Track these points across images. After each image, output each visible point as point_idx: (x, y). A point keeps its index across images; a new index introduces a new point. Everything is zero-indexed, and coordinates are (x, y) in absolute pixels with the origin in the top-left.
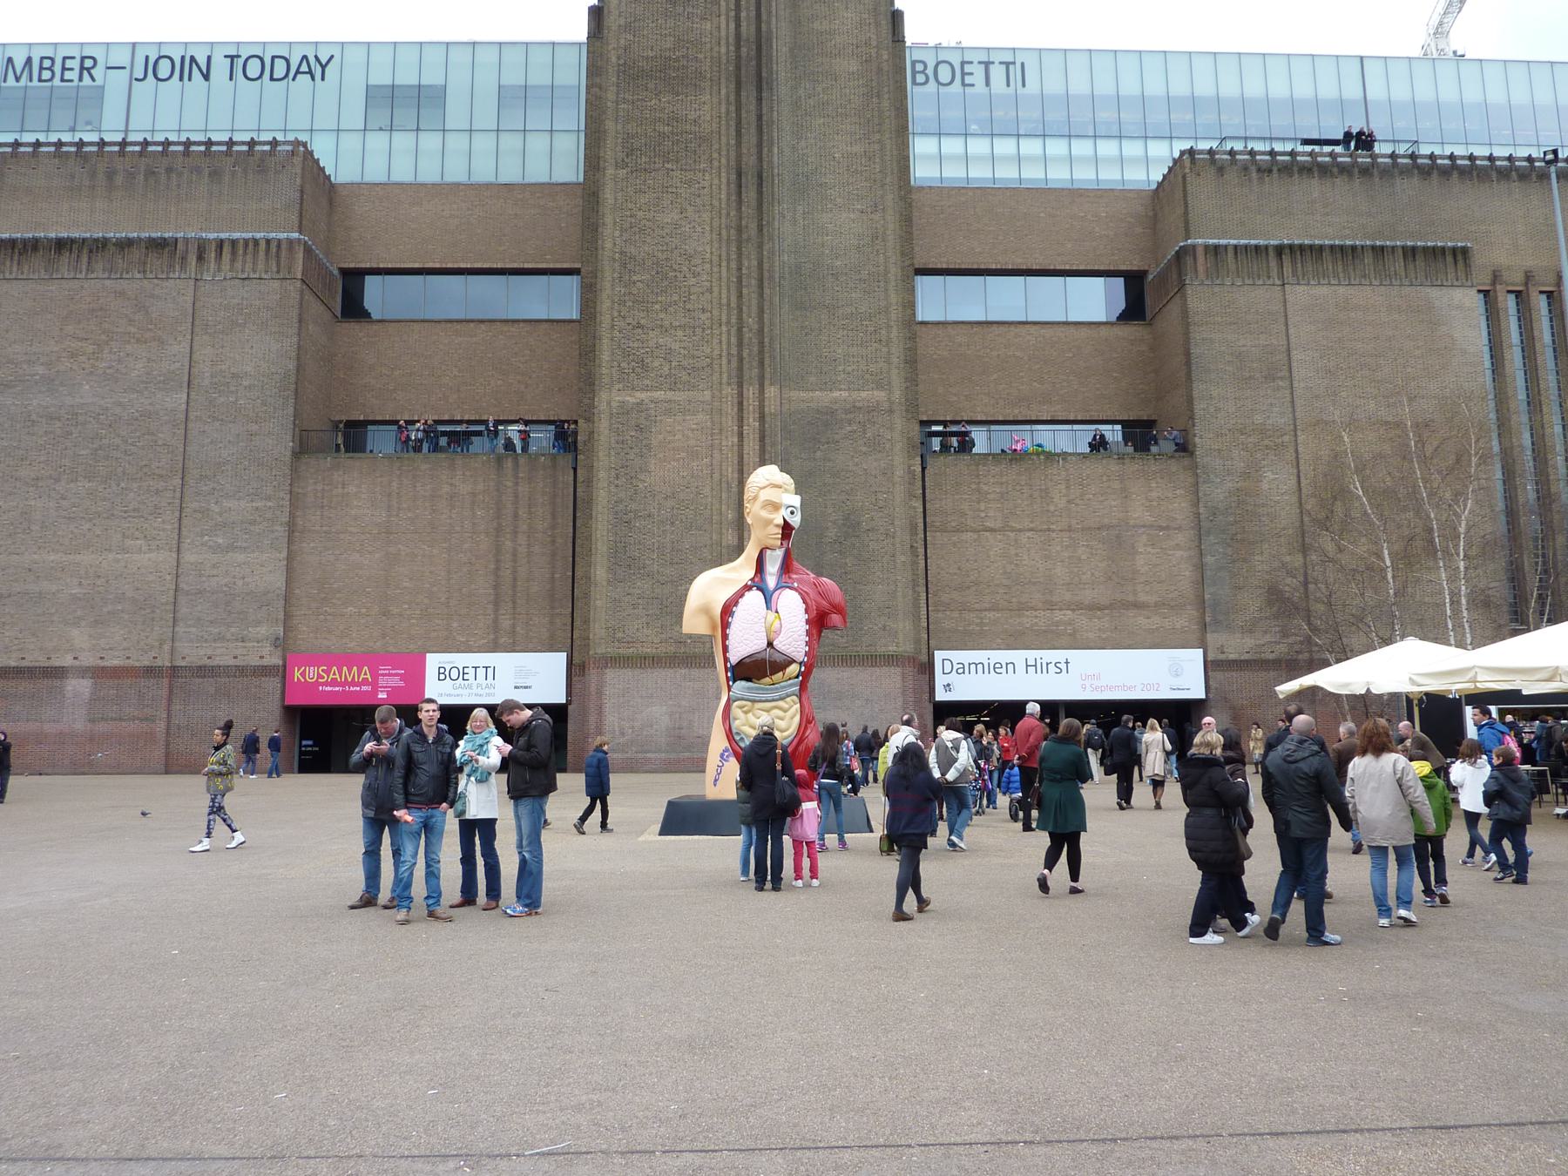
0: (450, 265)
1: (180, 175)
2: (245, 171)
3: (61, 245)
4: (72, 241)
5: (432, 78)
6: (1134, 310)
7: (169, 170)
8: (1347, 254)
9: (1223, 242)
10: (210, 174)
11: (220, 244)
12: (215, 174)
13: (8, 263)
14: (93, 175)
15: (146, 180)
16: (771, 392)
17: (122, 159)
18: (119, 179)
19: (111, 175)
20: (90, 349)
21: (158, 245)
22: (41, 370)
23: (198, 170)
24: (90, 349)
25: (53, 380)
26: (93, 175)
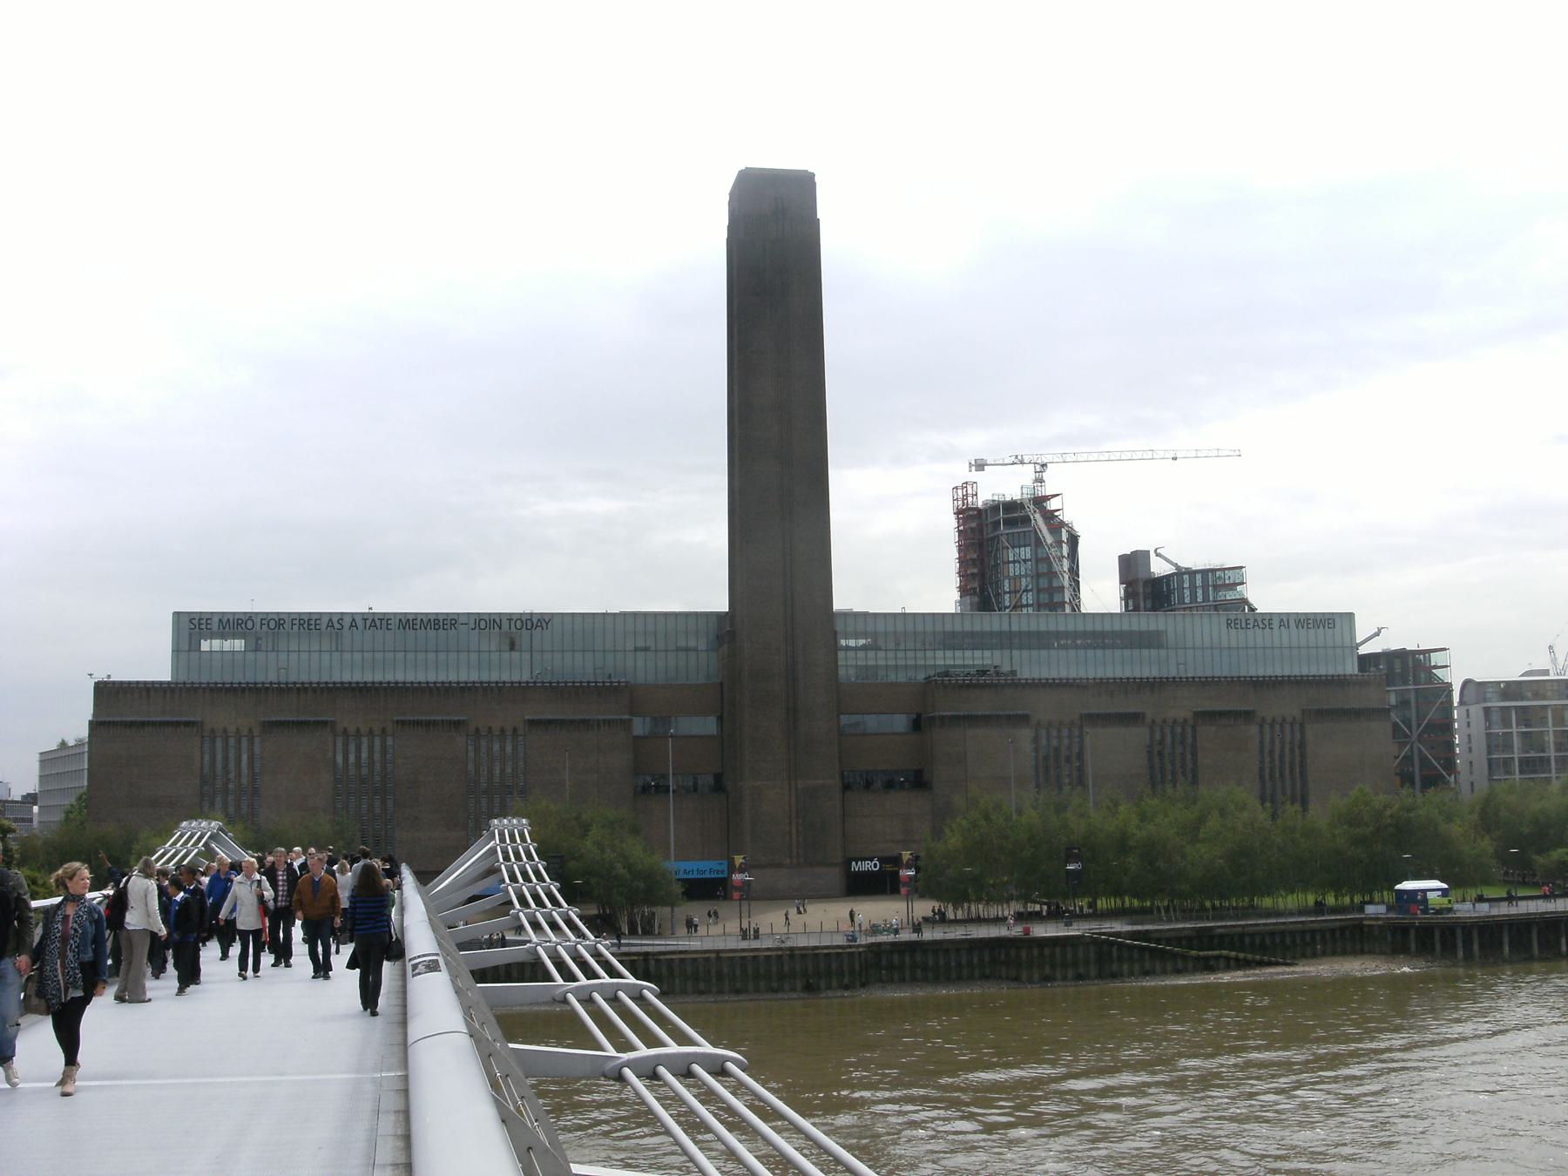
3: (550, 722)
6: (917, 724)
9: (944, 714)
11: (604, 720)
16: (799, 782)
21: (584, 722)
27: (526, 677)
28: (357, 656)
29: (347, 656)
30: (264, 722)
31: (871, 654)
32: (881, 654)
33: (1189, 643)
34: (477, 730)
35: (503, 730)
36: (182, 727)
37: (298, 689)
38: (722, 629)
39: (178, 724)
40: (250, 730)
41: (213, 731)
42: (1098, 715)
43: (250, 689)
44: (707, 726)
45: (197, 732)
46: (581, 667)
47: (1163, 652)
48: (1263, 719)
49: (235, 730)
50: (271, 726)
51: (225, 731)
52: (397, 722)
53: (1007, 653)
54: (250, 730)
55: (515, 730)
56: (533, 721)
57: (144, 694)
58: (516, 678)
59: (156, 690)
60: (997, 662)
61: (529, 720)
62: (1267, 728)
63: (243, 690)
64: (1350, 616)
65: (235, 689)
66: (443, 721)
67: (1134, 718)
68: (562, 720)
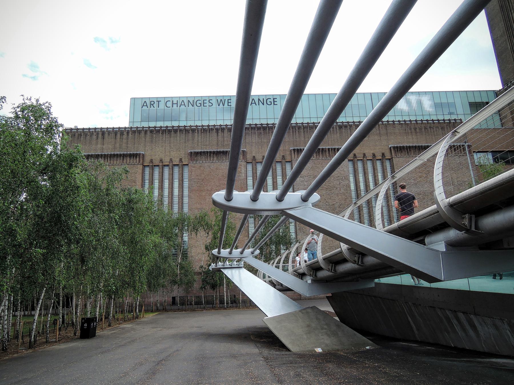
0: (485, 150)
1: (433, 129)
2: (450, 127)
4: (413, 147)
5: (451, 100)
7: (430, 127)
10: (441, 128)
12: (442, 128)
13: (397, 153)
14: (411, 129)
15: (425, 130)
17: (417, 125)
18: (418, 130)
19: (415, 129)
20: (425, 175)
22: (413, 181)
23: (438, 127)
24: (425, 175)
25: (417, 184)
26: (411, 129)
30: (191, 153)
35: (374, 155)
36: (128, 159)
37: (217, 130)
39: (124, 156)
40: (181, 160)
41: (151, 161)
43: (181, 130)
45: (139, 161)
49: (169, 161)
50: (195, 155)
51: (161, 161)
52: (294, 150)
54: (181, 160)
55: (383, 154)
56: (397, 147)
57: (100, 136)
59: (109, 132)
61: (394, 147)
63: (176, 131)
65: (170, 131)
66: (329, 149)
68: (419, 146)
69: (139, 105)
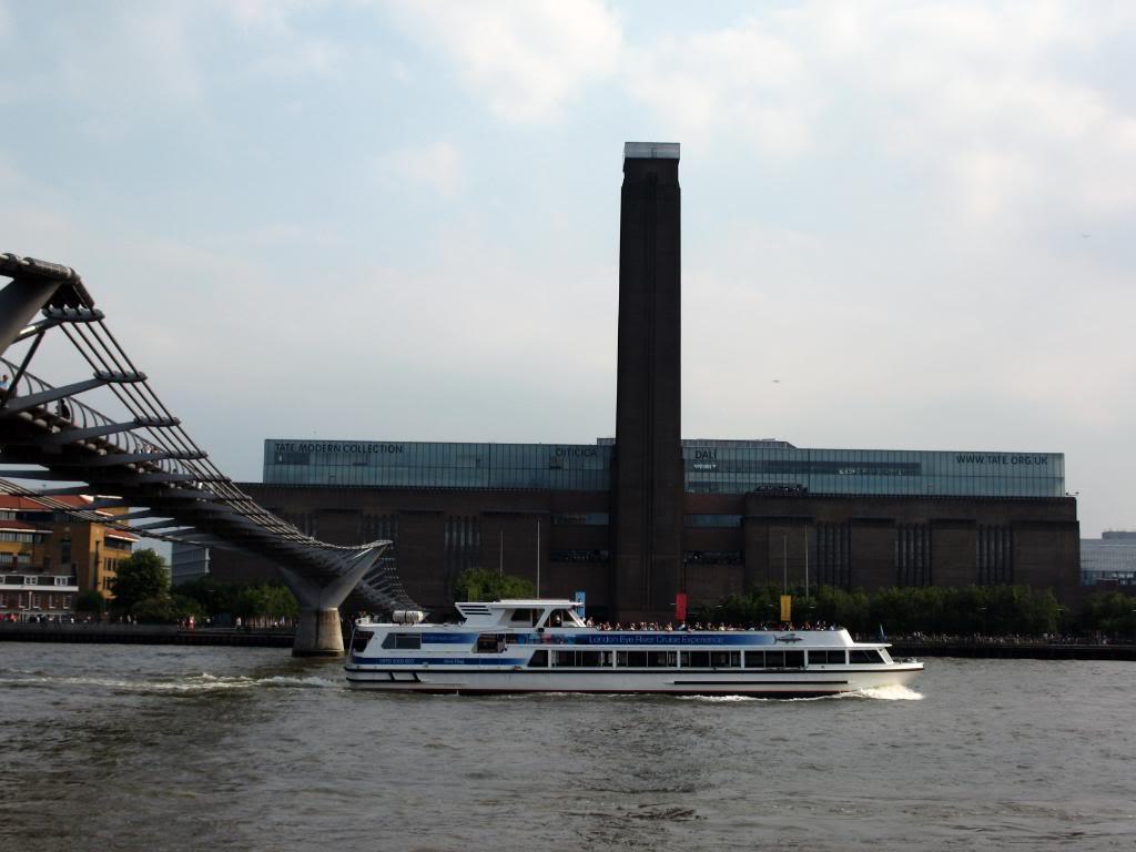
3: (498, 513)
8: (783, 518)
27: (486, 485)
28: (379, 469)
29: (373, 469)
31: (712, 475)
32: (719, 475)
33: (937, 472)
34: (451, 517)
38: (612, 453)
42: (862, 520)
44: (599, 519)
46: (522, 479)
47: (918, 478)
48: (981, 526)
53: (806, 476)
55: (474, 518)
58: (479, 484)
60: (799, 482)
62: (985, 533)
64: (1060, 456)
67: (885, 523)
69: (272, 445)
